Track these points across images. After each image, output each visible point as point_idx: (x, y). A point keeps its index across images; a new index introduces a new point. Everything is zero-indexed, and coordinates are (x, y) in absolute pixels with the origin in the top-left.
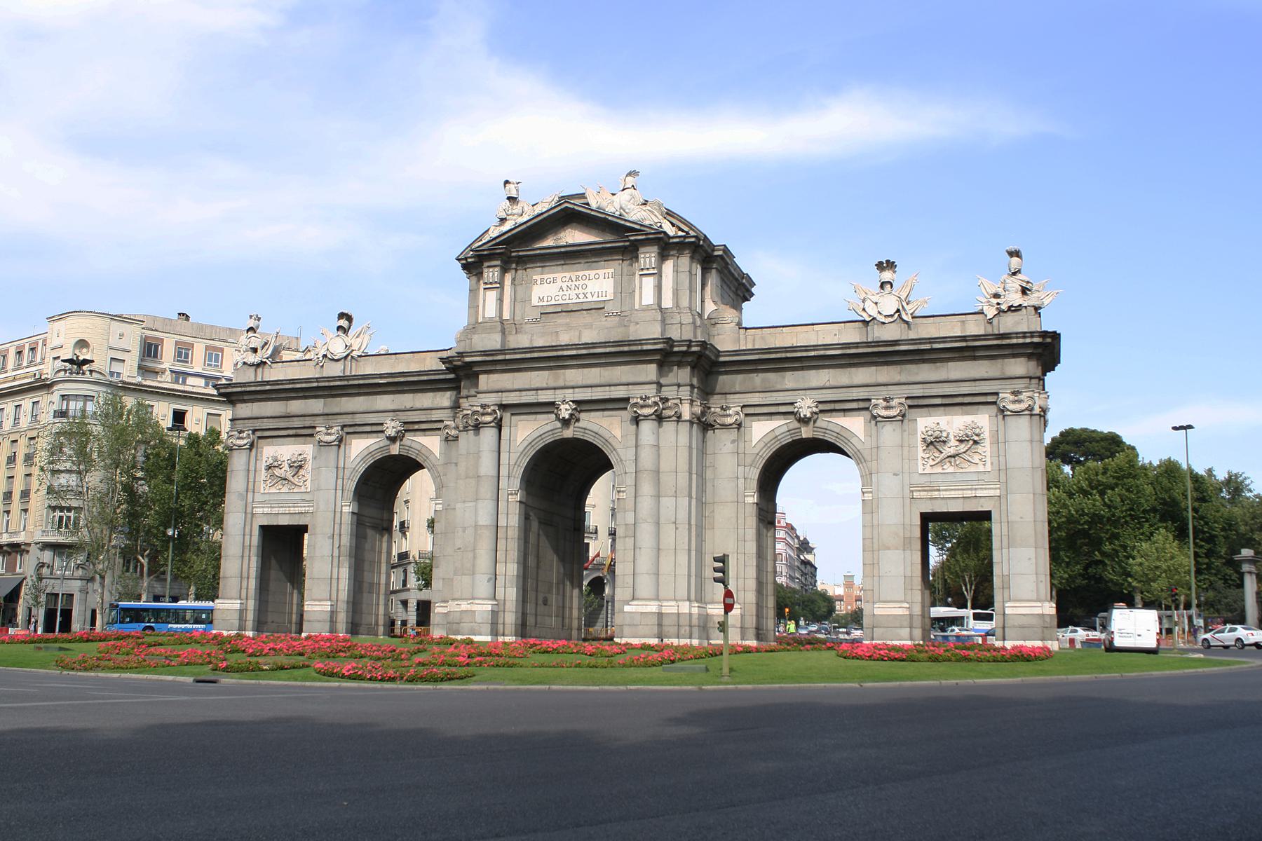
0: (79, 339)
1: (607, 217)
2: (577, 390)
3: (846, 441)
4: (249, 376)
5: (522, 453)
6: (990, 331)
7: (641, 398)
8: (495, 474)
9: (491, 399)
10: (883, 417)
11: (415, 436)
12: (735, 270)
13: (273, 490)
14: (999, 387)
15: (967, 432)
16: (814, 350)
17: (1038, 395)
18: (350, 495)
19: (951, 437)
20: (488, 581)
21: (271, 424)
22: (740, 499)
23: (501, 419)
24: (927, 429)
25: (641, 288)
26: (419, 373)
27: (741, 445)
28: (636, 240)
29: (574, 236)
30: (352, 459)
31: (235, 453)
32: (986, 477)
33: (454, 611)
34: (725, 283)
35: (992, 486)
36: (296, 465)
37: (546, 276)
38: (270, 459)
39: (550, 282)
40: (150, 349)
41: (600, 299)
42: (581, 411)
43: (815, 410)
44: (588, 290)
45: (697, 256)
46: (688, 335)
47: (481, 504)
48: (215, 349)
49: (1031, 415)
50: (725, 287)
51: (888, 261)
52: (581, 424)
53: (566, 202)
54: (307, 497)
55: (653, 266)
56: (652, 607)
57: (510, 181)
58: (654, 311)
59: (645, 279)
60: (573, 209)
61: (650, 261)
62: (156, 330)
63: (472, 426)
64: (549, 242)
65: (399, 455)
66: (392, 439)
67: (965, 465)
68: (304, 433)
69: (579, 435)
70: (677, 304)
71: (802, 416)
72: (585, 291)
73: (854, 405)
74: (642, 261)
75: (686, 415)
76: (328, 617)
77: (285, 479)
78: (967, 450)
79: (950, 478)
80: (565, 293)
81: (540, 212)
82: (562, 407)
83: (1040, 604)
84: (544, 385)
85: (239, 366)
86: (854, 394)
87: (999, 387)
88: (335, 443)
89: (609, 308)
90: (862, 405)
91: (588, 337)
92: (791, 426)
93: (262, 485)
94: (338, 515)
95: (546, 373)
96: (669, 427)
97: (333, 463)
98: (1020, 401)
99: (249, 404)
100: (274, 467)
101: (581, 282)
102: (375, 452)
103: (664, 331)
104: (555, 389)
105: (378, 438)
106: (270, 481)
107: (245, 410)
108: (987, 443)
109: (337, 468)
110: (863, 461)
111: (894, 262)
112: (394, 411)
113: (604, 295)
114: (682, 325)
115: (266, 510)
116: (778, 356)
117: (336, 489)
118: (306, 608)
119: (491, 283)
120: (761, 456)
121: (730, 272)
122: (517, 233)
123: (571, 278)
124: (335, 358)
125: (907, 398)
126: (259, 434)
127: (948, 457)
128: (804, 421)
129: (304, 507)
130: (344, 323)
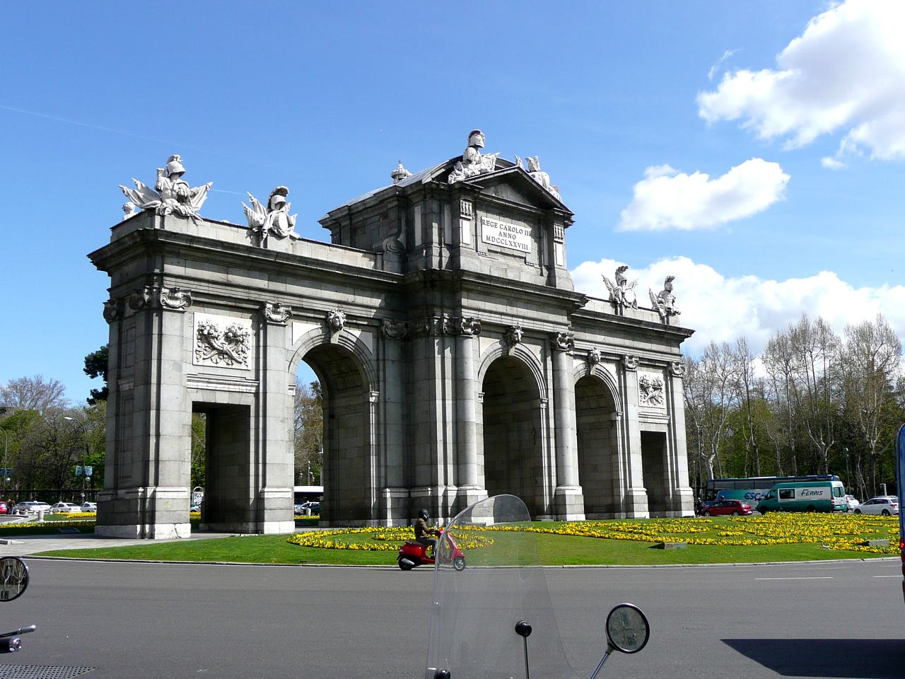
13: (208, 363)
15: (660, 383)
21: (211, 289)
29: (508, 196)
36: (241, 339)
37: (491, 220)
38: (208, 328)
43: (600, 357)
59: (558, 245)
77: (227, 354)
79: (650, 410)
80: (502, 238)
100: (214, 338)
102: (317, 338)
106: (205, 352)
115: (201, 385)
118: (266, 495)
119: (466, 214)
124: (284, 235)
130: (280, 198)
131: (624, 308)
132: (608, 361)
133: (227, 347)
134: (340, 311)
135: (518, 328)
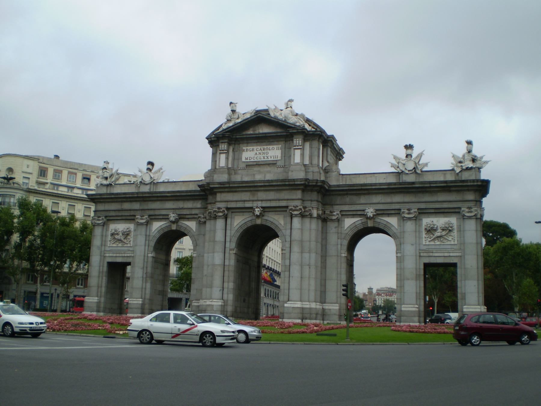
0: (7, 167)
1: (279, 121)
2: (263, 202)
3: (389, 229)
4: (104, 191)
5: (236, 231)
6: (457, 178)
7: (294, 206)
8: (224, 241)
9: (222, 205)
10: (407, 218)
11: (183, 221)
12: (336, 146)
14: (461, 205)
15: (447, 226)
16: (375, 186)
17: (479, 209)
18: (151, 249)
19: (439, 228)
20: (220, 291)
22: (339, 255)
23: (227, 215)
24: (427, 224)
25: (294, 155)
26: (187, 192)
27: (340, 229)
28: (292, 132)
30: (153, 231)
31: (96, 228)
32: (455, 247)
33: (203, 305)
34: (332, 152)
35: (457, 251)
36: (125, 233)
37: (248, 148)
39: (251, 151)
40: (43, 172)
41: (275, 159)
42: (265, 211)
43: (374, 213)
44: (269, 155)
45: (320, 140)
46: (317, 177)
47: (216, 255)
48: (72, 173)
49: (477, 219)
50: (332, 154)
51: (410, 145)
52: (265, 218)
53: (259, 113)
54: (131, 249)
55: (300, 144)
56: (298, 305)
57: (233, 102)
58: (300, 166)
59: (296, 151)
60: (263, 117)
61: (299, 142)
62: (44, 163)
63: (213, 217)
64: (250, 132)
65: (176, 230)
66: (173, 222)
67: (444, 241)
68: (131, 219)
69: (264, 223)
70: (311, 163)
71: (368, 216)
72: (267, 155)
73: (393, 212)
74: (295, 142)
75: (315, 215)
76: (140, 306)
77: (120, 240)
78: (446, 234)
79: (438, 247)
80: (258, 156)
81: (247, 118)
82: (256, 210)
83: (479, 307)
84: (248, 199)
85: (98, 186)
86: (393, 207)
87: (461, 205)
88: (145, 224)
89: (279, 163)
90: (396, 212)
91: (269, 177)
92: (363, 221)
93: (109, 243)
94: (146, 257)
95: (249, 193)
96: (307, 221)
97: (144, 233)
98: (471, 212)
99: (103, 204)
100: (115, 234)
101: (266, 151)
103: (306, 175)
104: (253, 201)
105: (166, 221)
107: (101, 207)
108: (455, 231)
109: (146, 235)
110: (397, 238)
111: (412, 145)
112: (173, 209)
113: (276, 157)
114: (313, 172)
115: (111, 255)
116: (358, 188)
117: (145, 246)
119: (223, 150)
120: (349, 235)
121: (334, 147)
122: (237, 127)
123: (261, 149)
125: (418, 209)
126: (108, 218)
127: (438, 237)
128: (370, 218)
129: (129, 253)
130: (150, 167)
131: (404, 175)
132: (389, 215)
133: (122, 238)
134: (173, 213)
135: (257, 207)
